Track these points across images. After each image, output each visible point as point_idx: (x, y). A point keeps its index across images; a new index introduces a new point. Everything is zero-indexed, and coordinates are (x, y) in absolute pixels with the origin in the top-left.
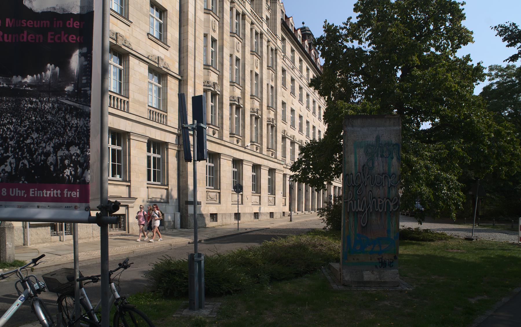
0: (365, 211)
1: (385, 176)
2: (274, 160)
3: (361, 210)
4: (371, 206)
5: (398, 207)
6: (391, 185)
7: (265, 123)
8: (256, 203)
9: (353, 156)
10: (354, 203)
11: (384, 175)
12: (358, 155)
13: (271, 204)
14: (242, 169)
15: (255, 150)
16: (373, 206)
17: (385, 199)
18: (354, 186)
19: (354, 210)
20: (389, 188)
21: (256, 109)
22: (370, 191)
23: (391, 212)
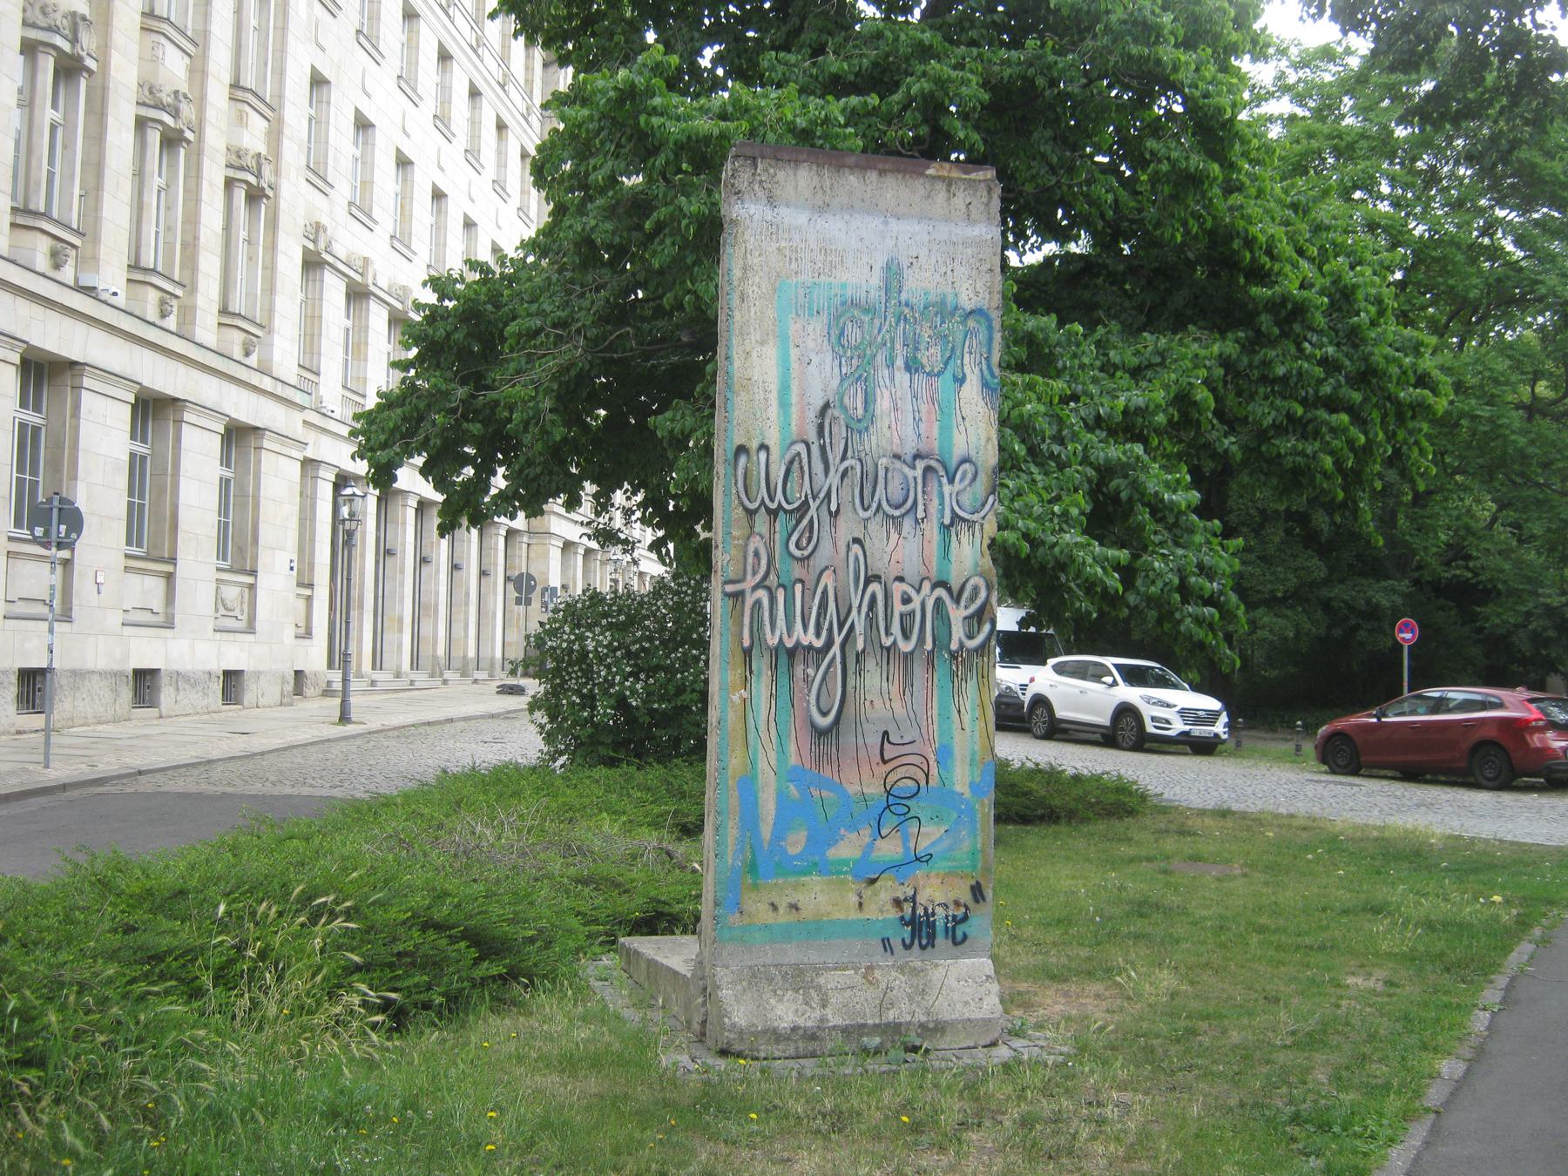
0: (829, 643)
2: (255, 379)
3: (809, 638)
4: (858, 620)
6: (955, 515)
7: (214, 173)
9: (771, 352)
11: (920, 465)
12: (794, 353)
13: (230, 623)
14: (76, 414)
16: (871, 621)
17: (927, 586)
19: (773, 641)
21: (168, 89)
22: (856, 541)
23: (954, 656)
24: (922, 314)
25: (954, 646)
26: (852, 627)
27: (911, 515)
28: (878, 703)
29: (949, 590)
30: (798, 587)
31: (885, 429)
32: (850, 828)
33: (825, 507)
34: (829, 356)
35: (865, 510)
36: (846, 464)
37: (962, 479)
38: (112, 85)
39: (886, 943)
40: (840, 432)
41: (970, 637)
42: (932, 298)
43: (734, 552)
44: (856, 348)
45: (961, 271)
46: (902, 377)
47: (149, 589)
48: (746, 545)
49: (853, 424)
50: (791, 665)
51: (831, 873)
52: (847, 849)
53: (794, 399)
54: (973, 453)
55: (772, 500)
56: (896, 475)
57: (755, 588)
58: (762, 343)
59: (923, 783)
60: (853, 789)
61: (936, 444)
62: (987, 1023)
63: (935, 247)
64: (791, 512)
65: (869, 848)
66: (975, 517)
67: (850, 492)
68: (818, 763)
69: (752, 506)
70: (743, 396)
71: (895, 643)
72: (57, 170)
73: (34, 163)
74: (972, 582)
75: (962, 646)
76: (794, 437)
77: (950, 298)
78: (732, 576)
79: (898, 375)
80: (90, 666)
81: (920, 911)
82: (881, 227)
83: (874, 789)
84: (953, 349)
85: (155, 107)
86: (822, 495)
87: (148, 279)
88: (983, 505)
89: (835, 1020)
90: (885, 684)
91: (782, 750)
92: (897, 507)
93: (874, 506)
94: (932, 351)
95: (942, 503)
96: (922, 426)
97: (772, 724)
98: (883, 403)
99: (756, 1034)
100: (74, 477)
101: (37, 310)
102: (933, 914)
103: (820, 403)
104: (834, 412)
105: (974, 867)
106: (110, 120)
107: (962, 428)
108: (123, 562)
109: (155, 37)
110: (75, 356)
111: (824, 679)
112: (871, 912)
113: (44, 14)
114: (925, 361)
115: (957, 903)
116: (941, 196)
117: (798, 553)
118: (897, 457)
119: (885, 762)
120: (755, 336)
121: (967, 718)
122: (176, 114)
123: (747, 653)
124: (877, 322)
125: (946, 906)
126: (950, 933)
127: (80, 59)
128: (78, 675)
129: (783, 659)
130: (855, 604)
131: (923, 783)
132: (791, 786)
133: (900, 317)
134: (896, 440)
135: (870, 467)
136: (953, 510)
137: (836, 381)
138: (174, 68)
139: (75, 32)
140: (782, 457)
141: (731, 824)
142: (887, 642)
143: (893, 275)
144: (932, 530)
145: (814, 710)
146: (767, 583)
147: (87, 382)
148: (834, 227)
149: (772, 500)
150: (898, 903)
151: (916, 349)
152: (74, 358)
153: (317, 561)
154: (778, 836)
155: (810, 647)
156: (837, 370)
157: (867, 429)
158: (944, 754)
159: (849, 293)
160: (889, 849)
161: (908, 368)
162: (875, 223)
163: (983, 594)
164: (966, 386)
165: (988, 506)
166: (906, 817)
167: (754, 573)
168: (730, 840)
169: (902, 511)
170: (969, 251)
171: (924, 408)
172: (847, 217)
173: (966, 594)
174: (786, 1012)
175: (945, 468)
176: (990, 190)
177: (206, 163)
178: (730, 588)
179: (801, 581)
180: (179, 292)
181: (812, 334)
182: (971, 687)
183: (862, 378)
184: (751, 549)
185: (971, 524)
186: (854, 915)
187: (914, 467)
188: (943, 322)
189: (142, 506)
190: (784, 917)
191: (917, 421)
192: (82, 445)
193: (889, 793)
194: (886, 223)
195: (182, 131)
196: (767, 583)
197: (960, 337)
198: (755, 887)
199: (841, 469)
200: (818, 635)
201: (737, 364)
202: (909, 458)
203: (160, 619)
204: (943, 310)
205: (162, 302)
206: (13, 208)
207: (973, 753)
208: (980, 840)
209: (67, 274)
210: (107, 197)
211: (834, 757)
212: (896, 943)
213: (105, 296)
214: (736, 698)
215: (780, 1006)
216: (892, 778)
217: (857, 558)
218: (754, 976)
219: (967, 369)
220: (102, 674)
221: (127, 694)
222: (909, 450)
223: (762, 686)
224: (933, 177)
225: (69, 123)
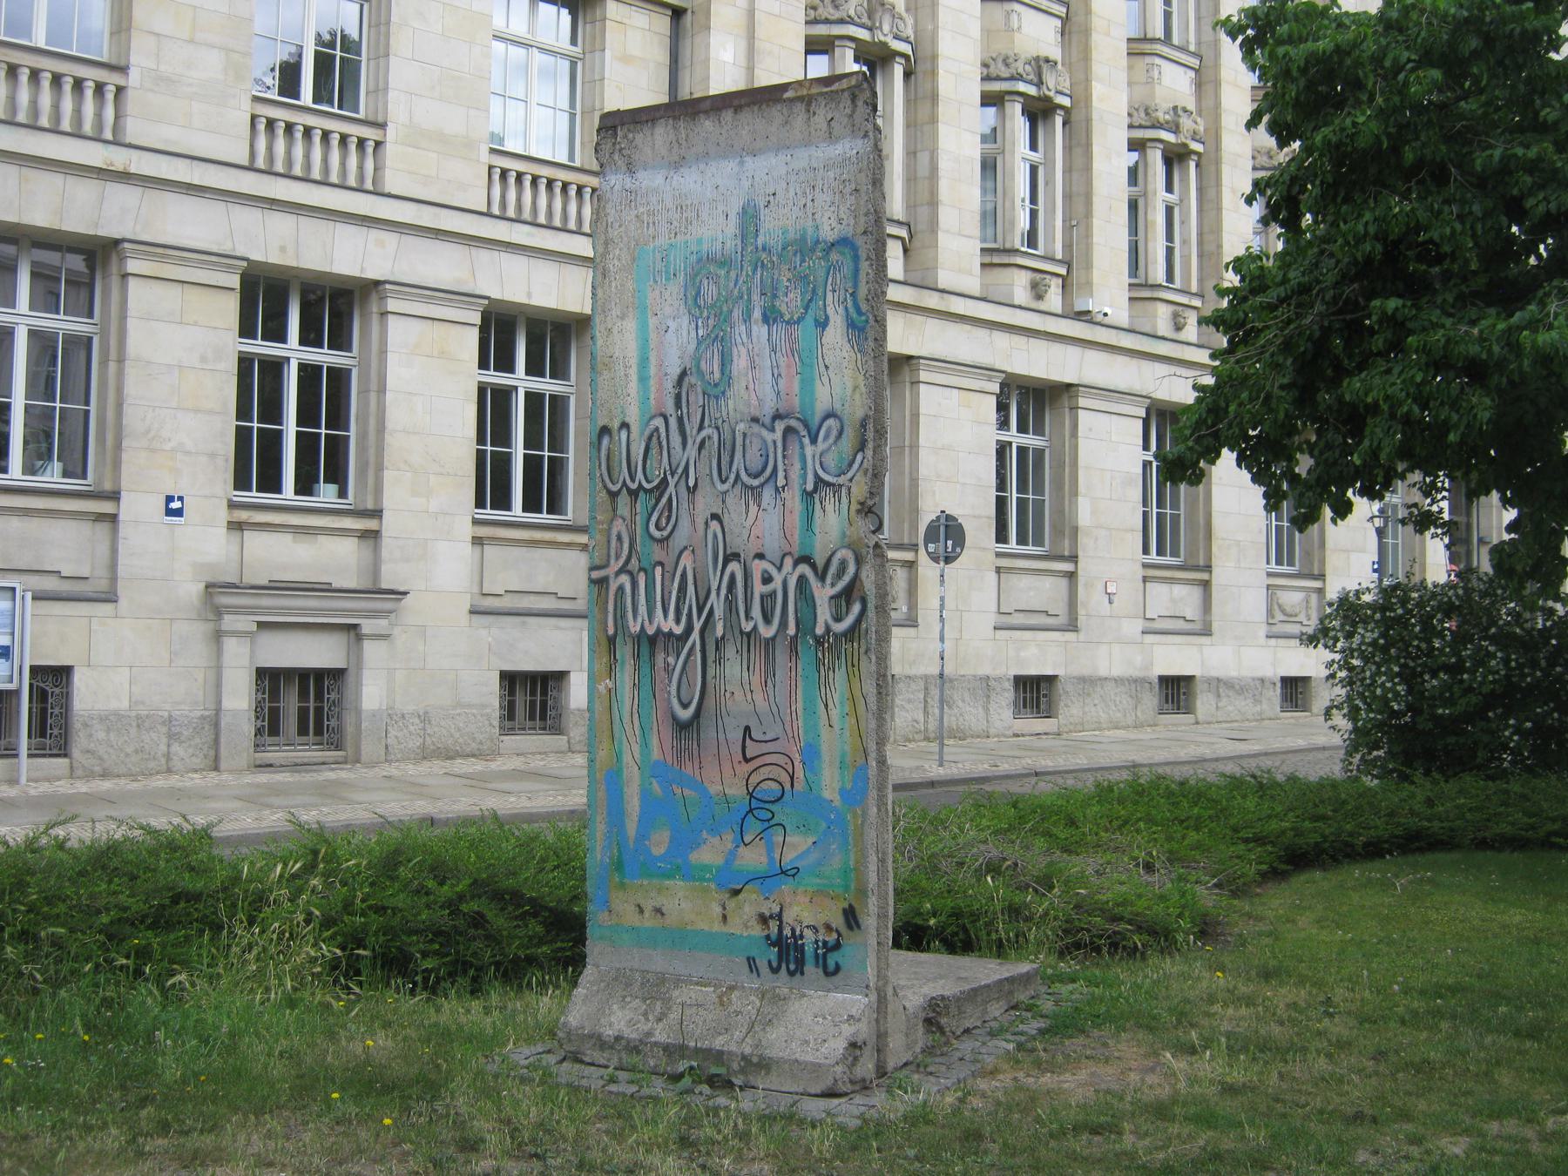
1: (789, 431)
3: (669, 625)
4: (717, 603)
6: (819, 481)
9: (630, 325)
10: (634, 584)
11: (780, 426)
12: (652, 322)
15: (1164, 326)
17: (789, 561)
18: (634, 494)
19: (635, 628)
20: (808, 496)
22: (715, 517)
23: (819, 641)
24: (780, 256)
25: (819, 631)
27: (771, 484)
28: (739, 695)
29: (813, 566)
30: (659, 570)
31: (743, 391)
32: (713, 831)
33: (683, 482)
34: (685, 320)
35: (723, 482)
36: (704, 433)
37: (826, 437)
38: (1095, 116)
39: (751, 963)
40: (697, 399)
41: (838, 619)
42: (791, 236)
43: (598, 537)
44: (712, 306)
45: (823, 198)
46: (760, 331)
47: (1178, 598)
49: (709, 389)
50: (652, 654)
51: (693, 879)
52: (709, 854)
53: (653, 370)
54: (838, 406)
55: (633, 480)
56: (755, 440)
57: (618, 573)
58: (622, 318)
59: (787, 786)
60: (714, 789)
61: (797, 401)
62: (816, 1067)
63: (793, 178)
65: (732, 855)
66: (841, 480)
67: (708, 465)
68: (681, 754)
69: (615, 488)
70: (606, 375)
71: (755, 628)
72: (1041, 207)
73: (1007, 204)
74: (839, 555)
75: (828, 629)
76: (653, 411)
77: (810, 231)
78: (597, 562)
79: (755, 328)
80: (1103, 672)
81: (787, 932)
82: (736, 169)
83: (736, 790)
84: (814, 291)
85: (1153, 127)
86: (680, 471)
87: (1156, 294)
88: (851, 465)
89: (660, 1036)
90: (745, 674)
91: (645, 744)
92: (756, 477)
93: (732, 477)
94: (791, 295)
95: (804, 468)
96: (782, 382)
98: (740, 363)
99: (584, 1038)
102: (802, 937)
103: (678, 371)
104: (691, 379)
105: (847, 888)
106: (1096, 149)
108: (1140, 572)
109: (1148, 59)
111: (684, 668)
112: (735, 927)
113: (1007, 65)
114: (783, 308)
115: (828, 928)
116: (799, 119)
117: (657, 534)
118: (755, 420)
119: (747, 760)
120: (616, 312)
121: (835, 713)
122: (1176, 129)
123: (612, 641)
124: (733, 274)
125: (815, 929)
126: (821, 961)
127: (1048, 99)
128: (1088, 683)
129: (645, 650)
130: (714, 587)
131: (787, 786)
132: (654, 781)
133: (758, 264)
134: (754, 402)
135: (727, 436)
137: (693, 346)
138: (1175, 84)
139: (1040, 76)
141: (599, 818)
142: (747, 627)
143: (749, 218)
144: (794, 499)
145: (675, 701)
146: (629, 567)
148: (690, 181)
149: (633, 480)
150: (764, 920)
151: (775, 296)
152: (1068, 380)
153: (1429, 560)
154: (642, 836)
155: (670, 634)
156: (693, 334)
158: (811, 754)
159: (705, 248)
160: (753, 858)
162: (730, 166)
163: (851, 569)
164: (829, 330)
165: (856, 466)
166: (770, 824)
167: (617, 557)
168: (599, 835)
169: (760, 481)
170: (831, 174)
171: (783, 361)
172: (702, 166)
173: (833, 570)
174: (621, 1020)
175: (806, 426)
176: (854, 98)
177: (1226, 170)
178: (596, 575)
179: (661, 564)
180: (1197, 303)
181: (669, 301)
182: (840, 676)
183: (718, 340)
184: (614, 532)
185: (836, 488)
186: (717, 927)
188: (803, 261)
189: (1175, 519)
190: (649, 921)
191: (776, 377)
192: (1081, 463)
193: (751, 795)
194: (742, 163)
195: (1185, 145)
196: (629, 567)
197: (821, 273)
198: (622, 886)
199: (698, 440)
200: (678, 621)
201: (599, 342)
202: (767, 420)
203: (1197, 626)
204: (803, 247)
205: (1176, 315)
206: (982, 250)
208: (852, 857)
209: (1054, 300)
210: (1096, 223)
211: (696, 753)
212: (762, 964)
213: (1100, 318)
214: (601, 688)
215: (620, 1014)
216: (754, 780)
217: (715, 536)
218: (616, 979)
219: (830, 311)
220: (1118, 681)
221: (1151, 700)
223: (626, 675)
224: (792, 100)
225: (1049, 161)
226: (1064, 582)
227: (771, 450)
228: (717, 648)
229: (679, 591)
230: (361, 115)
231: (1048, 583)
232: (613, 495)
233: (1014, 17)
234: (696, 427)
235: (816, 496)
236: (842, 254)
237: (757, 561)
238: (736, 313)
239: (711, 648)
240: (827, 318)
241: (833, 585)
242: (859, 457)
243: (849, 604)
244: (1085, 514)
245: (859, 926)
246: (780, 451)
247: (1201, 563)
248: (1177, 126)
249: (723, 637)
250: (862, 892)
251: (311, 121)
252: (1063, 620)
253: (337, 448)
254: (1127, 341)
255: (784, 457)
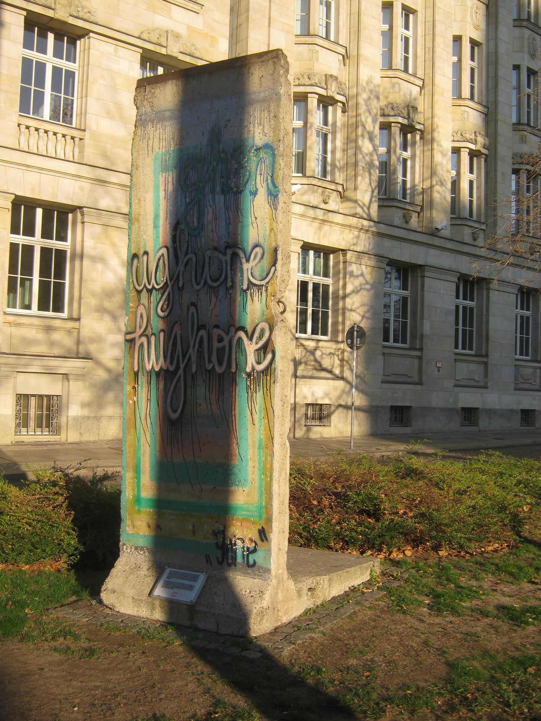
0: (178, 368)
4: (193, 354)
5: (269, 356)
6: (250, 283)
8: (473, 383)
15: (468, 239)
16: (200, 353)
18: (150, 291)
19: (149, 367)
22: (193, 304)
23: (249, 375)
25: (248, 370)
26: (190, 359)
29: (246, 332)
35: (198, 284)
41: (259, 363)
46: (220, 198)
47: (469, 370)
48: (136, 312)
54: (261, 241)
55: (149, 284)
64: (159, 290)
66: (263, 283)
69: (139, 288)
71: (213, 368)
75: (253, 369)
78: (129, 330)
79: (217, 197)
80: (434, 405)
86: (175, 278)
87: (464, 223)
88: (268, 275)
90: (207, 394)
92: (215, 281)
96: (231, 227)
97: (148, 417)
98: (209, 216)
100: (422, 318)
101: (397, 243)
102: (235, 544)
104: (183, 226)
105: (260, 517)
107: (255, 225)
108: (453, 357)
110: (420, 262)
114: (233, 185)
115: (251, 540)
118: (216, 249)
121: (256, 417)
123: (136, 374)
128: (426, 410)
136: (249, 279)
139: (408, 114)
140: (155, 257)
142: (209, 367)
145: (169, 409)
146: (147, 333)
147: (427, 274)
149: (149, 284)
150: (215, 534)
152: (419, 263)
156: (183, 200)
157: (199, 234)
161: (223, 192)
167: (140, 328)
173: (256, 335)
177: (499, 163)
178: (129, 337)
180: (483, 227)
185: (260, 287)
187: (225, 254)
189: (471, 332)
192: (426, 303)
196: (147, 333)
200: (172, 363)
202: (222, 249)
203: (482, 384)
207: (261, 440)
217: (193, 315)
219: (259, 186)
220: (443, 409)
221: (457, 420)
222: (223, 244)
226: (416, 361)
227: (224, 266)
228: (192, 379)
229: (173, 346)
230: (74, 126)
231: (408, 361)
232: (139, 292)
233: (397, 86)
234: (184, 253)
235: (249, 292)
236: (266, 153)
237: (215, 330)
238: (207, 189)
239: (189, 379)
240: (257, 190)
241: (256, 343)
242: (273, 269)
243: (265, 353)
244: (427, 327)
245: (267, 540)
246: (229, 267)
247: (484, 353)
248: (476, 141)
249: (196, 373)
250: (269, 520)
251: (48, 127)
252: (416, 379)
253: (59, 289)
254: (449, 245)
255: (231, 270)
